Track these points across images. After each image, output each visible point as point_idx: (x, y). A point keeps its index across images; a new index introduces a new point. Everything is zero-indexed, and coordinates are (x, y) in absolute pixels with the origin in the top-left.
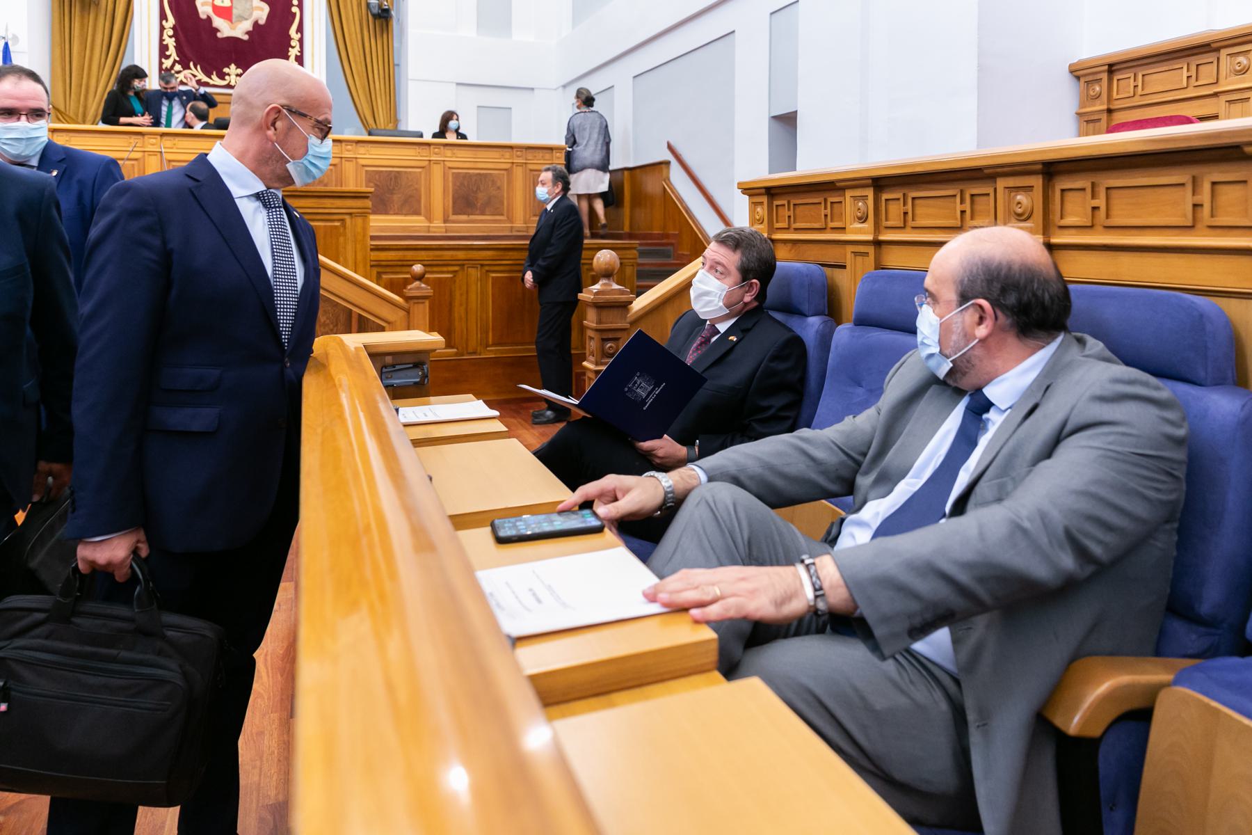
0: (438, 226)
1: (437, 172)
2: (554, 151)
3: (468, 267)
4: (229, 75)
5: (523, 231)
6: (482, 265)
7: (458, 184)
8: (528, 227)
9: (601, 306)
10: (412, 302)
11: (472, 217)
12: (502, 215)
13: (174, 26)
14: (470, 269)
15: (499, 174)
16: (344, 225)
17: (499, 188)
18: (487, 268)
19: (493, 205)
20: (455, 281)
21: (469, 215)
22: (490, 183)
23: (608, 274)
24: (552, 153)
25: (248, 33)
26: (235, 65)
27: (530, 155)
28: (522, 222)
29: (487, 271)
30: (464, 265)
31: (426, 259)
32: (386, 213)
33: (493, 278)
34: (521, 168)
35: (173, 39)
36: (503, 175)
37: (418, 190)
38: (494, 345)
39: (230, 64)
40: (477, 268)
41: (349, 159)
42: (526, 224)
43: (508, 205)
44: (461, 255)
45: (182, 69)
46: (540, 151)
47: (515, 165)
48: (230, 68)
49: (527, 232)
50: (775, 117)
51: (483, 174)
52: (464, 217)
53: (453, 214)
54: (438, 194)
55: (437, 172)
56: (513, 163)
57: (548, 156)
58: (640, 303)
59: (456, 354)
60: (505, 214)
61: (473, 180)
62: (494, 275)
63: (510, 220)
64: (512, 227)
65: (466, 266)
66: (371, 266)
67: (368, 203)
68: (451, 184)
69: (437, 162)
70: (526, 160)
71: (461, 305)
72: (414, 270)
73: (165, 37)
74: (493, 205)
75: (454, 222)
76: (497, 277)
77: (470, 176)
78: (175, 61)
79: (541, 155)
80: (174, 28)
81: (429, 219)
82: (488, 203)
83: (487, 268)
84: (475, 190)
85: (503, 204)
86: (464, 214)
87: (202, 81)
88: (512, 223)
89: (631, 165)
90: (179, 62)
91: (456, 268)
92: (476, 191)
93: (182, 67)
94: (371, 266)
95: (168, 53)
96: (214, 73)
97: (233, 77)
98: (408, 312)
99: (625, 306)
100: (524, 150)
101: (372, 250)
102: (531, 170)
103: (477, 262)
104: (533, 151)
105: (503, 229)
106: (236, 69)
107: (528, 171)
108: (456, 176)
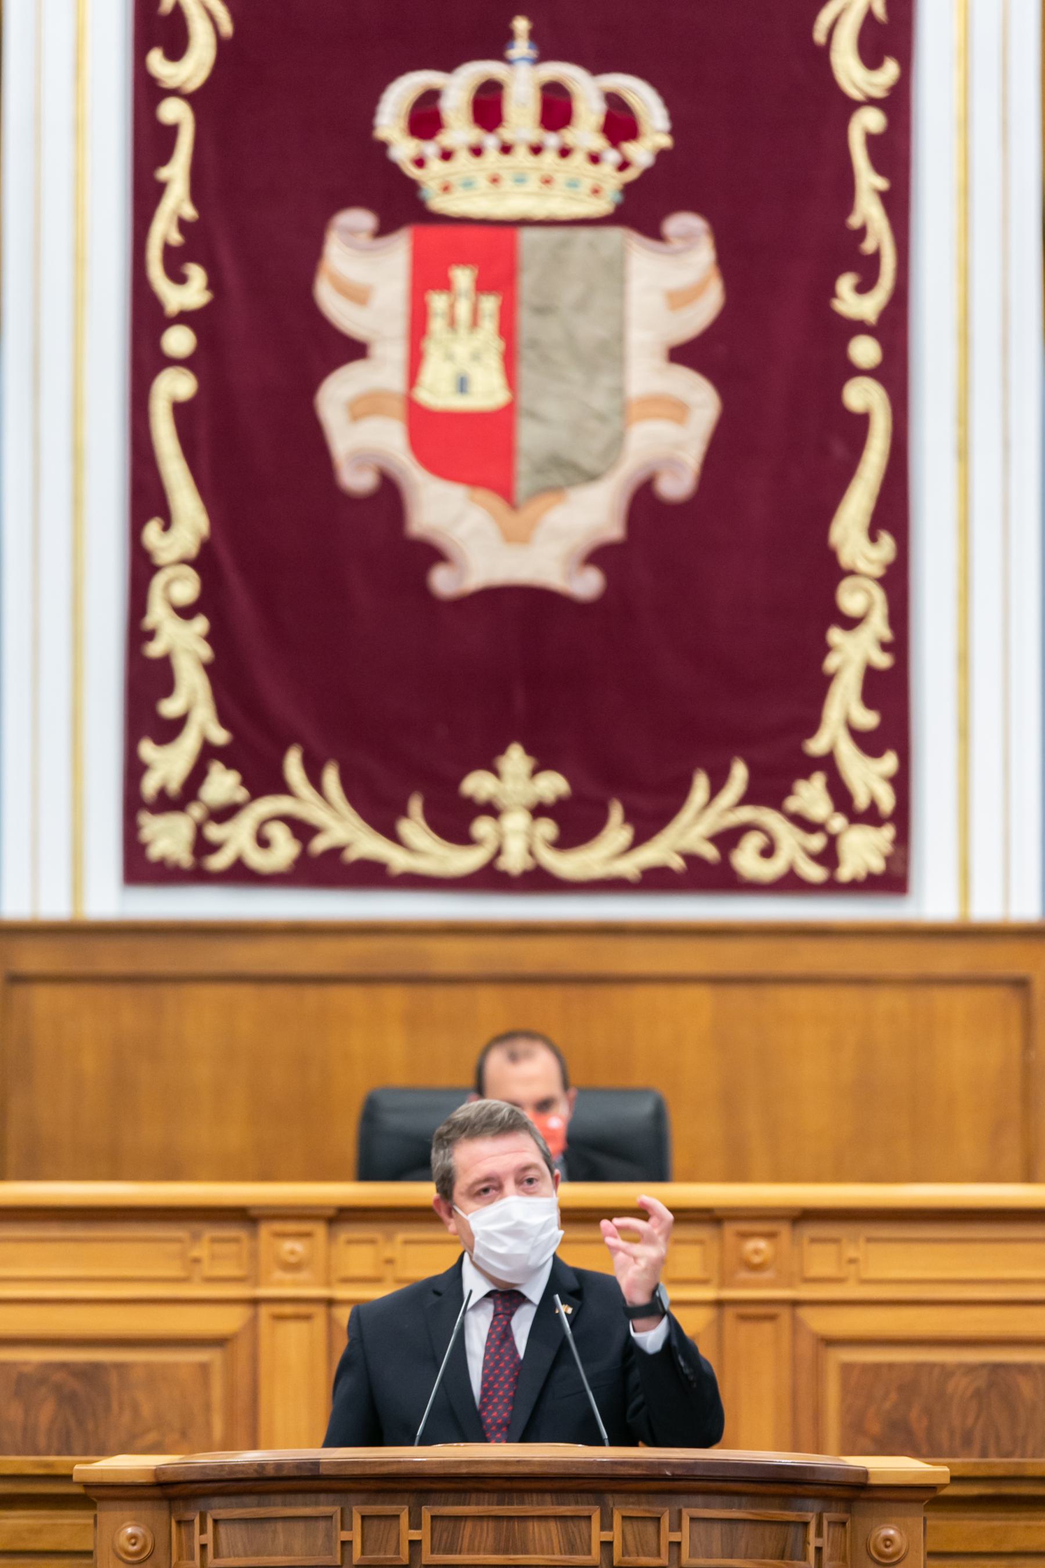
4: (491, 810)
13: (206, 547)
26: (529, 751)
35: (201, 624)
39: (502, 750)
45: (241, 794)
48: (496, 773)
73: (158, 614)
78: (208, 753)
87: (352, 855)
90: (228, 756)
93: (245, 783)
95: (170, 708)
96: (416, 806)
97: (516, 821)
106: (535, 772)
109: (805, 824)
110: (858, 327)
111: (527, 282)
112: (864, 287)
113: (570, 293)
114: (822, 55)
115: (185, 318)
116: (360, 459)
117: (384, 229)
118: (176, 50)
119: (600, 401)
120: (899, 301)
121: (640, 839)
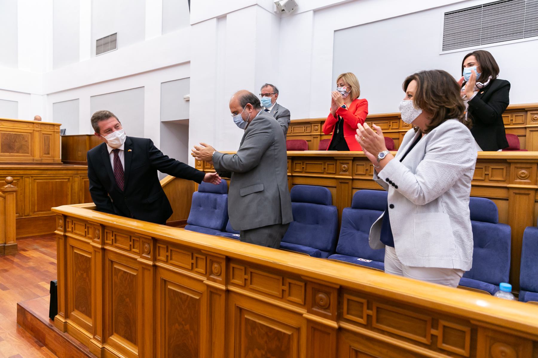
2: (55, 126)
3: (25, 178)
5: (40, 161)
6: (32, 177)
7: (4, 138)
8: (42, 159)
10: (7, 194)
11: (12, 154)
12: (29, 153)
14: (25, 178)
15: (27, 135)
18: (35, 178)
19: (23, 149)
20: (18, 184)
21: (10, 153)
22: (22, 139)
24: (54, 127)
27: (43, 127)
28: (39, 157)
29: (34, 179)
30: (23, 177)
31: (3, 174)
33: (37, 182)
34: (38, 132)
36: (29, 135)
38: (38, 211)
40: (30, 178)
42: (40, 158)
43: (31, 150)
44: (21, 172)
46: (48, 126)
47: (35, 131)
49: (41, 161)
50: (162, 122)
51: (18, 134)
56: (34, 130)
57: (52, 128)
59: (19, 216)
60: (30, 153)
61: (13, 137)
62: (38, 181)
63: (32, 155)
64: (33, 159)
65: (24, 177)
70: (41, 129)
71: (21, 194)
72: (7, 179)
74: (23, 149)
76: (40, 182)
77: (11, 135)
79: (48, 127)
83: (35, 178)
84: (13, 141)
85: (28, 148)
86: (7, 152)
88: (34, 157)
89: (89, 134)
91: (18, 178)
92: (14, 142)
98: (5, 198)
100: (40, 125)
102: (43, 134)
103: (29, 175)
104: (45, 125)
107: (42, 134)
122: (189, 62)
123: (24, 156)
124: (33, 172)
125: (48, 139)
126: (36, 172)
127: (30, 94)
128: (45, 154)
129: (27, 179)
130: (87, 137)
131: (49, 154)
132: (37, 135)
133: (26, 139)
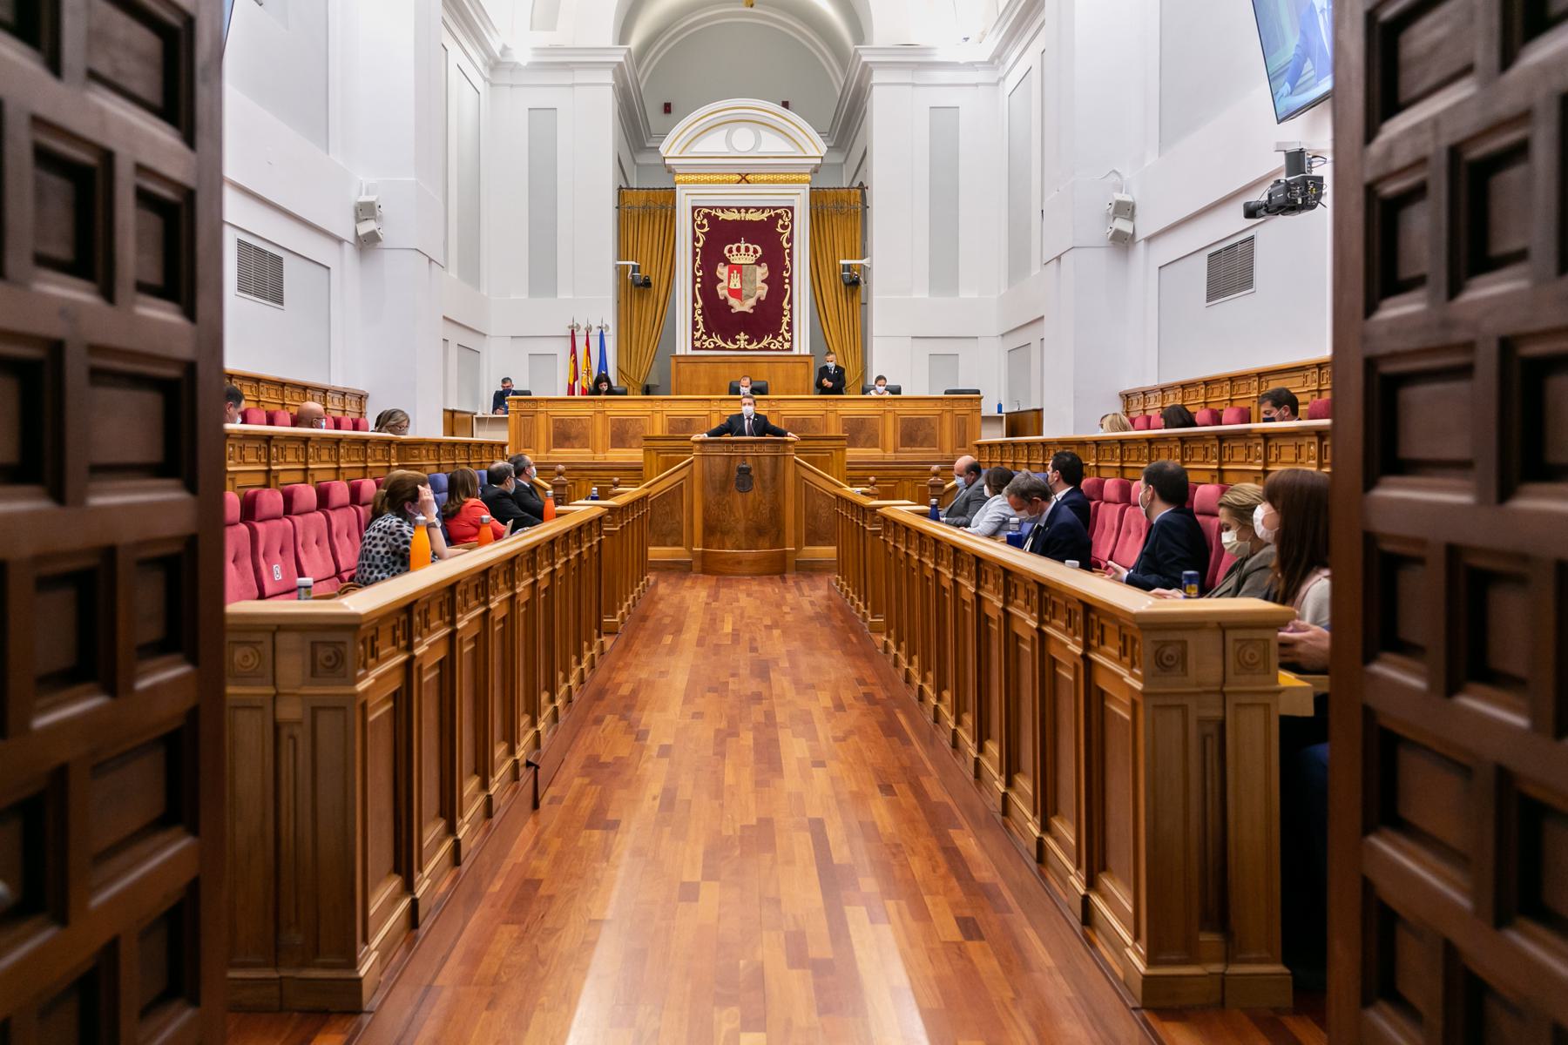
0: (890, 455)
1: (890, 417)
4: (739, 340)
6: (913, 479)
9: (933, 486)
11: (914, 449)
16: (832, 456)
17: (933, 428)
23: (936, 474)
25: (753, 307)
32: (856, 447)
37: (877, 431)
41: (832, 411)
44: (899, 473)
52: (908, 449)
53: (901, 446)
54: (890, 434)
55: (890, 417)
57: (969, 404)
58: (948, 486)
63: (941, 450)
66: (847, 479)
67: (845, 443)
68: (899, 426)
69: (890, 411)
75: (900, 452)
77: (913, 420)
80: (702, 308)
81: (885, 452)
82: (925, 439)
85: (935, 438)
90: (705, 333)
94: (847, 479)
99: (942, 487)
101: (848, 470)
105: (935, 457)
108: (902, 420)
109: (778, 341)
110: (787, 278)
111: (743, 271)
112: (787, 273)
113: (749, 274)
114: (782, 242)
115: (700, 277)
116: (722, 295)
117: (725, 265)
118: (698, 242)
119: (753, 287)
120: (792, 274)
121: (758, 344)
122: (1042, 318)
123: (929, 451)
124: (913, 472)
125: (964, 421)
126: (918, 472)
127: (977, 338)
128: (960, 447)
129: (906, 483)
130: (1034, 413)
131: (965, 446)
132: (947, 417)
133: (933, 425)
